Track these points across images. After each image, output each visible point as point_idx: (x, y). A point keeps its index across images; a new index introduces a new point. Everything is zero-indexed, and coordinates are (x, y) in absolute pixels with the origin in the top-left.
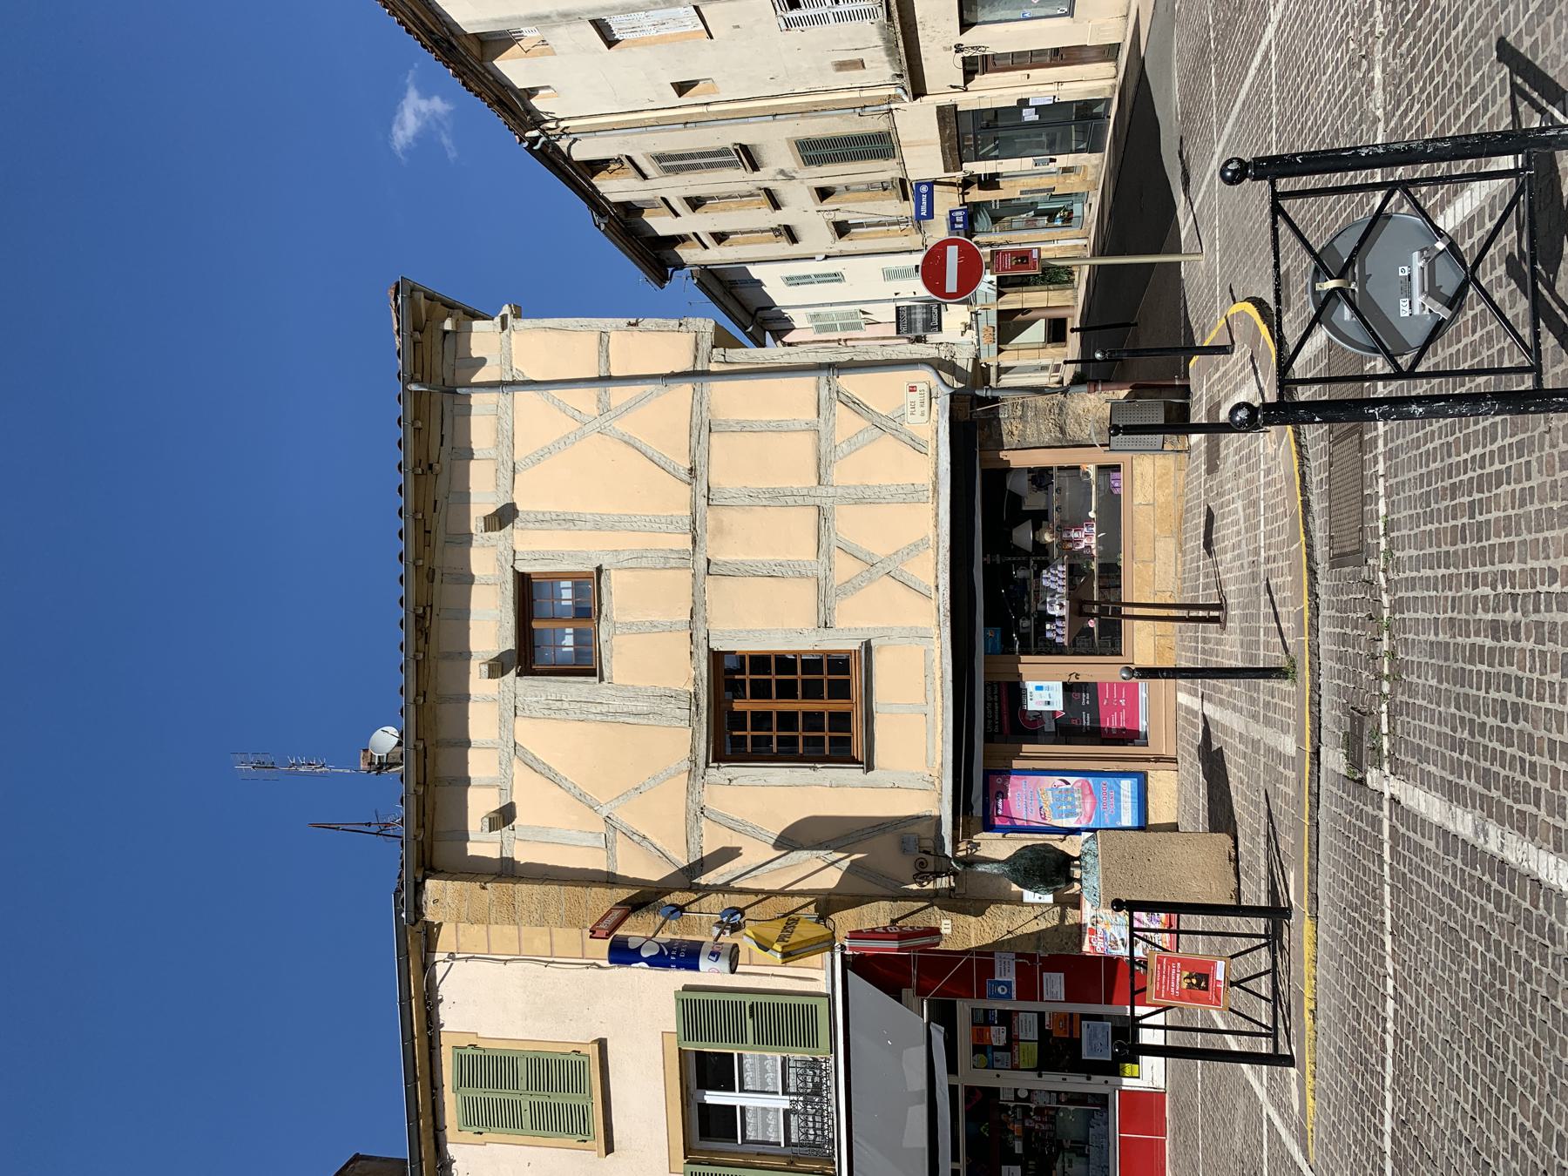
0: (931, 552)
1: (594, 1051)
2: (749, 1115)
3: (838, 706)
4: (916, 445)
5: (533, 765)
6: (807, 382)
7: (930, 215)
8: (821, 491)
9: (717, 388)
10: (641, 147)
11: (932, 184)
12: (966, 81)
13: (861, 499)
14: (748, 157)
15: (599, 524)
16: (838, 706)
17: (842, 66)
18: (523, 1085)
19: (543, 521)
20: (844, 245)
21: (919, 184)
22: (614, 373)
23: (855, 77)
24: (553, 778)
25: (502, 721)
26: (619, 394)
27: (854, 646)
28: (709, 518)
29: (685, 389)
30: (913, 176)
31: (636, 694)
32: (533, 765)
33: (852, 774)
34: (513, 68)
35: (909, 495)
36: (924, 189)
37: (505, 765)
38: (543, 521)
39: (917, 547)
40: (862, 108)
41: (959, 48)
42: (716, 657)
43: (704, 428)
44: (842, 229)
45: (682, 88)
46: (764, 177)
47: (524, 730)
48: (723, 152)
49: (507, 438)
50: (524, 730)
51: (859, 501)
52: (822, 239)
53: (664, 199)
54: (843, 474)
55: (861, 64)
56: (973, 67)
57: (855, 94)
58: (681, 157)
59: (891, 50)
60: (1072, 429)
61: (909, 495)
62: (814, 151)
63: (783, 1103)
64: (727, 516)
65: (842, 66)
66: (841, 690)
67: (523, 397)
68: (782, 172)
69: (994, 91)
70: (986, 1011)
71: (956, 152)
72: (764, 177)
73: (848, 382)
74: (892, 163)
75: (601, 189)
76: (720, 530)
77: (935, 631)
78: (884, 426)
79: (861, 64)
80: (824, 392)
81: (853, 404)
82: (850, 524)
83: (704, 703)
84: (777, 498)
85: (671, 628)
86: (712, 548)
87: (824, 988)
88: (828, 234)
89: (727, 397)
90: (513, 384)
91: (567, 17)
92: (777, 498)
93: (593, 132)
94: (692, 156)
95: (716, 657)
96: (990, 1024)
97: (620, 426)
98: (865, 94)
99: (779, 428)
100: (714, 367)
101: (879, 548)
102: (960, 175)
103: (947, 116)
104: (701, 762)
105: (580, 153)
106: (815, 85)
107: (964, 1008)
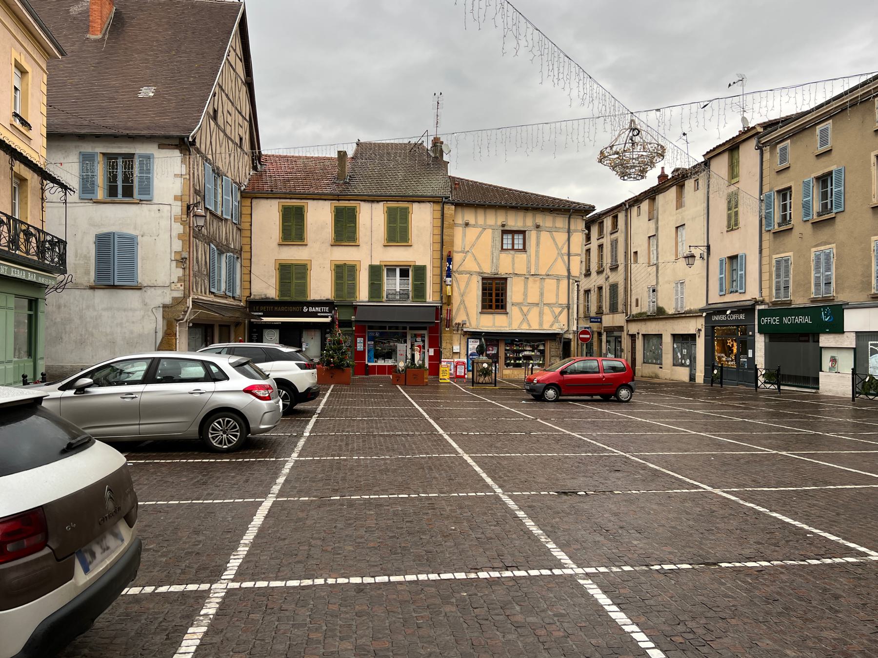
0: (528, 328)
1: (410, 243)
2: (394, 281)
3: (494, 306)
4: (552, 325)
5: (481, 233)
6: (567, 303)
7: (591, 322)
8: (542, 304)
9: (565, 282)
10: (620, 236)
11: (601, 322)
12: (630, 335)
13: (541, 314)
14: (614, 268)
15: (537, 252)
16: (494, 306)
17: (637, 300)
18: (401, 225)
19: (538, 238)
20: (582, 292)
21: (601, 319)
22: (571, 257)
23: (634, 304)
24: (478, 237)
25: (490, 226)
26: (566, 258)
27: (508, 311)
28: (538, 278)
29: (566, 274)
30: (604, 317)
31: (498, 259)
32: (481, 233)
33: (480, 310)
34: (645, 205)
35: (541, 324)
36: (599, 320)
37: (481, 226)
38: (538, 238)
39: (529, 325)
40: (626, 305)
41: (638, 333)
42: (506, 279)
43: (558, 279)
44: (587, 292)
45: (636, 253)
46: (607, 271)
47: (489, 232)
48: (616, 261)
49: (557, 230)
50: (489, 232)
51: (540, 313)
52: (585, 284)
53: (603, 237)
54: (546, 310)
55: (637, 306)
56: (633, 337)
57: (629, 303)
58: (616, 248)
59: (641, 314)
60: (553, 358)
61: (541, 324)
62: (614, 288)
63: (398, 290)
64: (538, 283)
65: (637, 300)
66: (497, 307)
67: (565, 236)
68: (608, 277)
69: (626, 343)
70: (424, 337)
71: (610, 330)
72: (607, 271)
73: (566, 310)
74: (608, 311)
75: (608, 218)
76: (535, 281)
77: (511, 328)
78: (556, 318)
79: (637, 306)
80: (564, 306)
81: (560, 313)
82: (535, 311)
83: (496, 276)
84: (542, 294)
85: (513, 269)
86: (531, 279)
87: (427, 300)
88: (586, 287)
89: (564, 283)
90: (569, 232)
91: (657, 229)
92: (542, 294)
93: (626, 224)
94: (616, 251)
95: (506, 279)
96: (422, 337)
97: (560, 260)
98: (629, 306)
99: (557, 295)
100: (571, 281)
101: (529, 317)
102: (603, 331)
103: (621, 328)
104: (482, 275)
105: (621, 217)
106: (633, 292)
107: (425, 332)
